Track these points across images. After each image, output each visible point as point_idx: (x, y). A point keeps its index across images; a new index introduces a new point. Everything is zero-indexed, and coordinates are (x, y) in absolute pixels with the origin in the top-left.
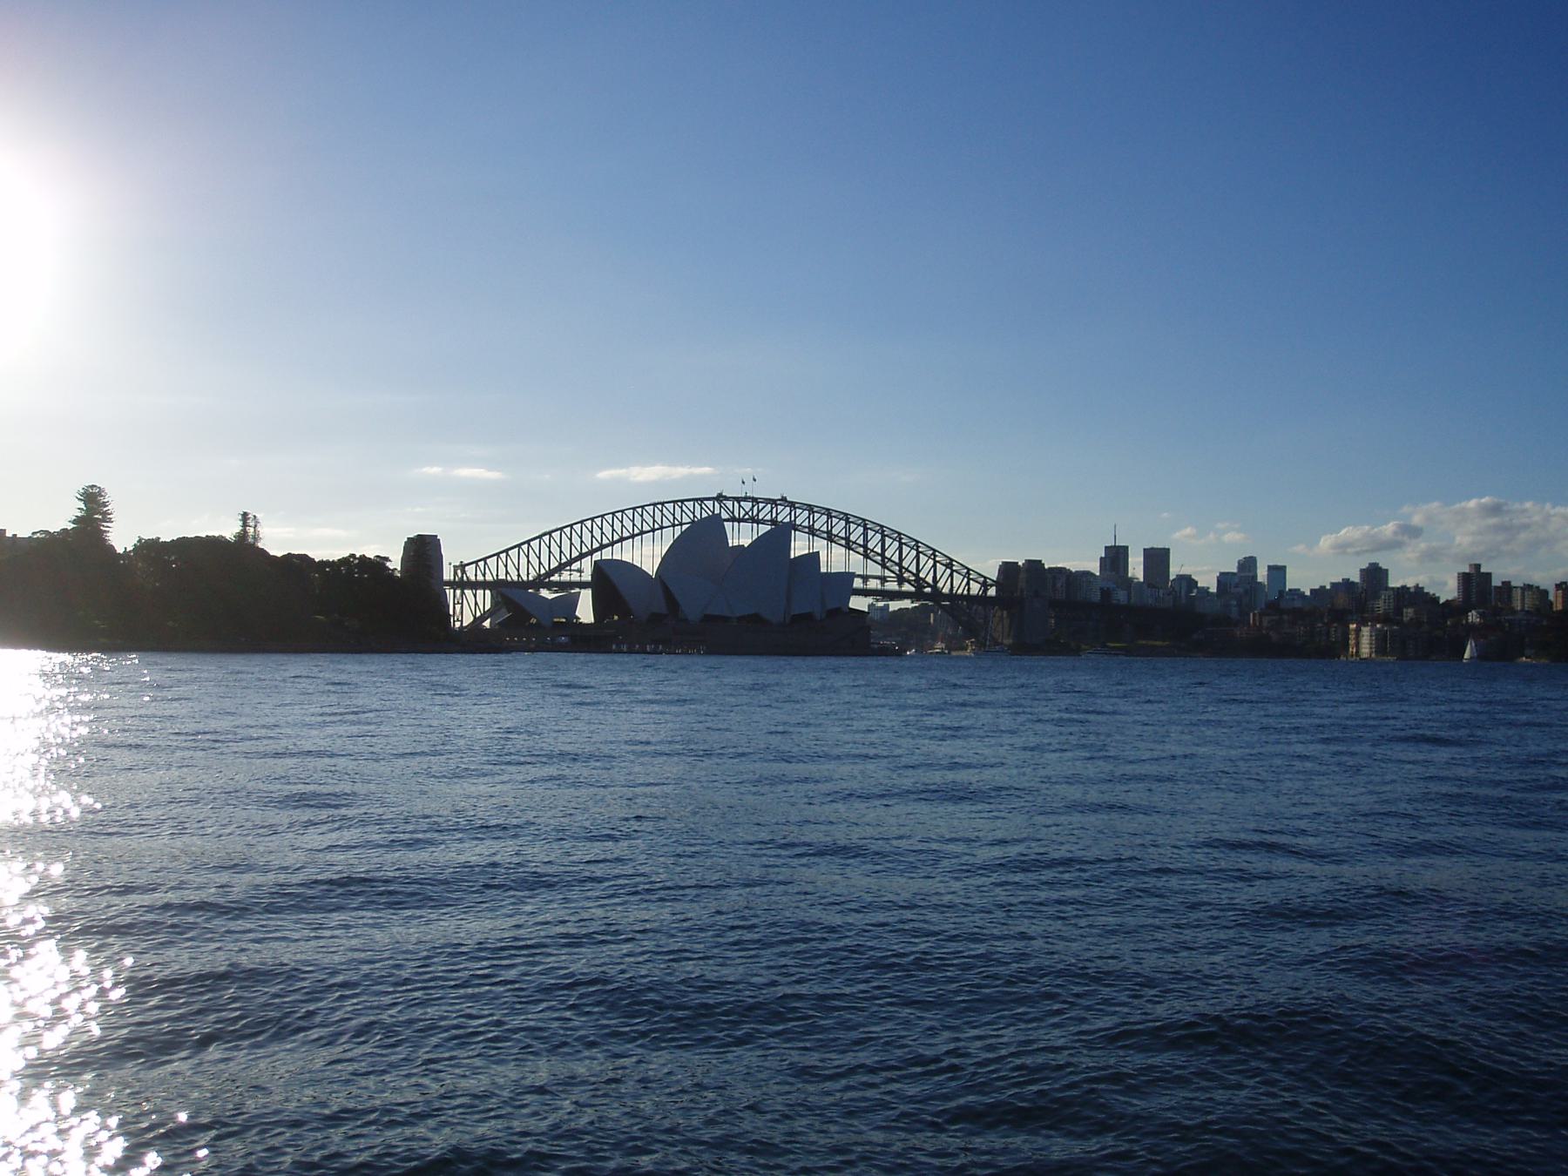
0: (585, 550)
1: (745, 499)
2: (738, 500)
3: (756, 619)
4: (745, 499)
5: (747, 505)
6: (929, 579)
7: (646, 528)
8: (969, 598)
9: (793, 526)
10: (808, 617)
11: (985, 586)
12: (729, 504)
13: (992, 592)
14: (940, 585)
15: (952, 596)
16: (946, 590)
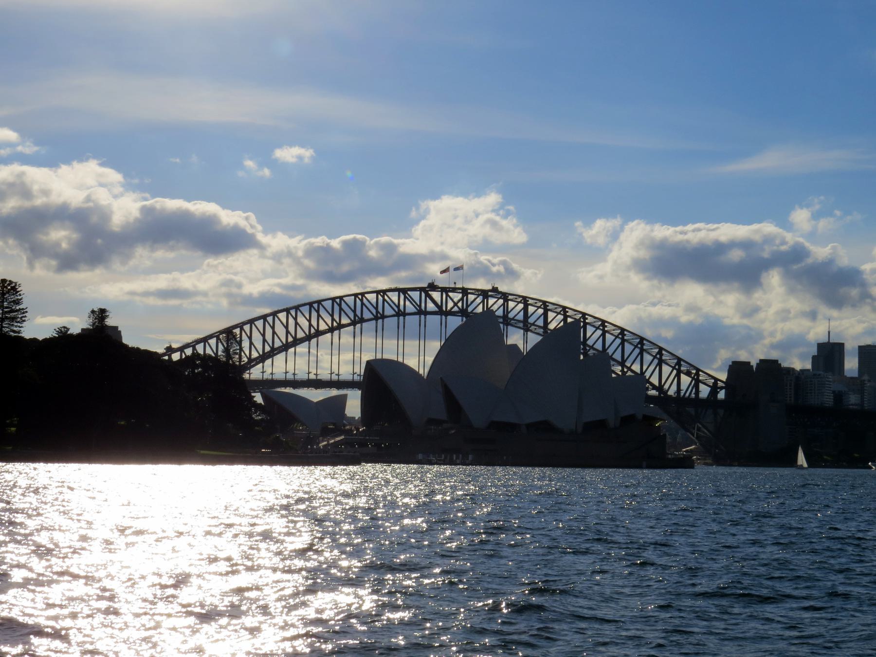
0: (278, 344)
1: (454, 290)
2: (445, 290)
3: (544, 427)
4: (454, 290)
5: (457, 296)
6: (655, 380)
7: (345, 321)
8: (697, 402)
9: (507, 320)
10: (601, 424)
11: (714, 389)
12: (436, 295)
13: (721, 395)
14: (666, 387)
15: (680, 400)
16: (671, 392)
